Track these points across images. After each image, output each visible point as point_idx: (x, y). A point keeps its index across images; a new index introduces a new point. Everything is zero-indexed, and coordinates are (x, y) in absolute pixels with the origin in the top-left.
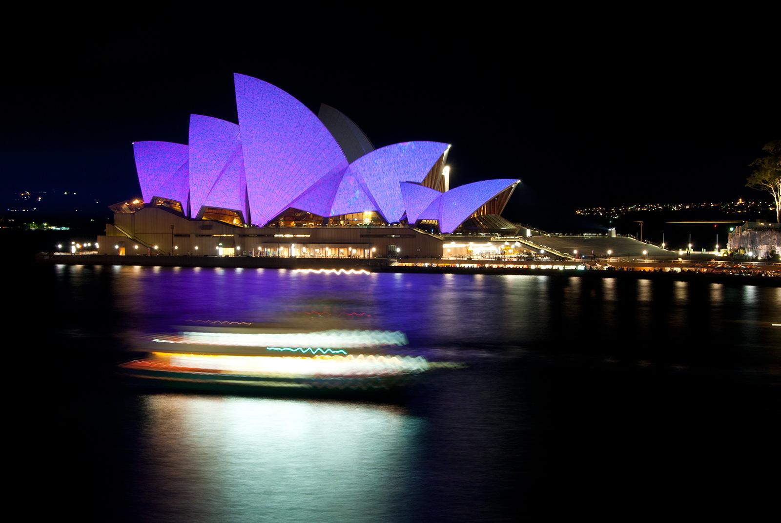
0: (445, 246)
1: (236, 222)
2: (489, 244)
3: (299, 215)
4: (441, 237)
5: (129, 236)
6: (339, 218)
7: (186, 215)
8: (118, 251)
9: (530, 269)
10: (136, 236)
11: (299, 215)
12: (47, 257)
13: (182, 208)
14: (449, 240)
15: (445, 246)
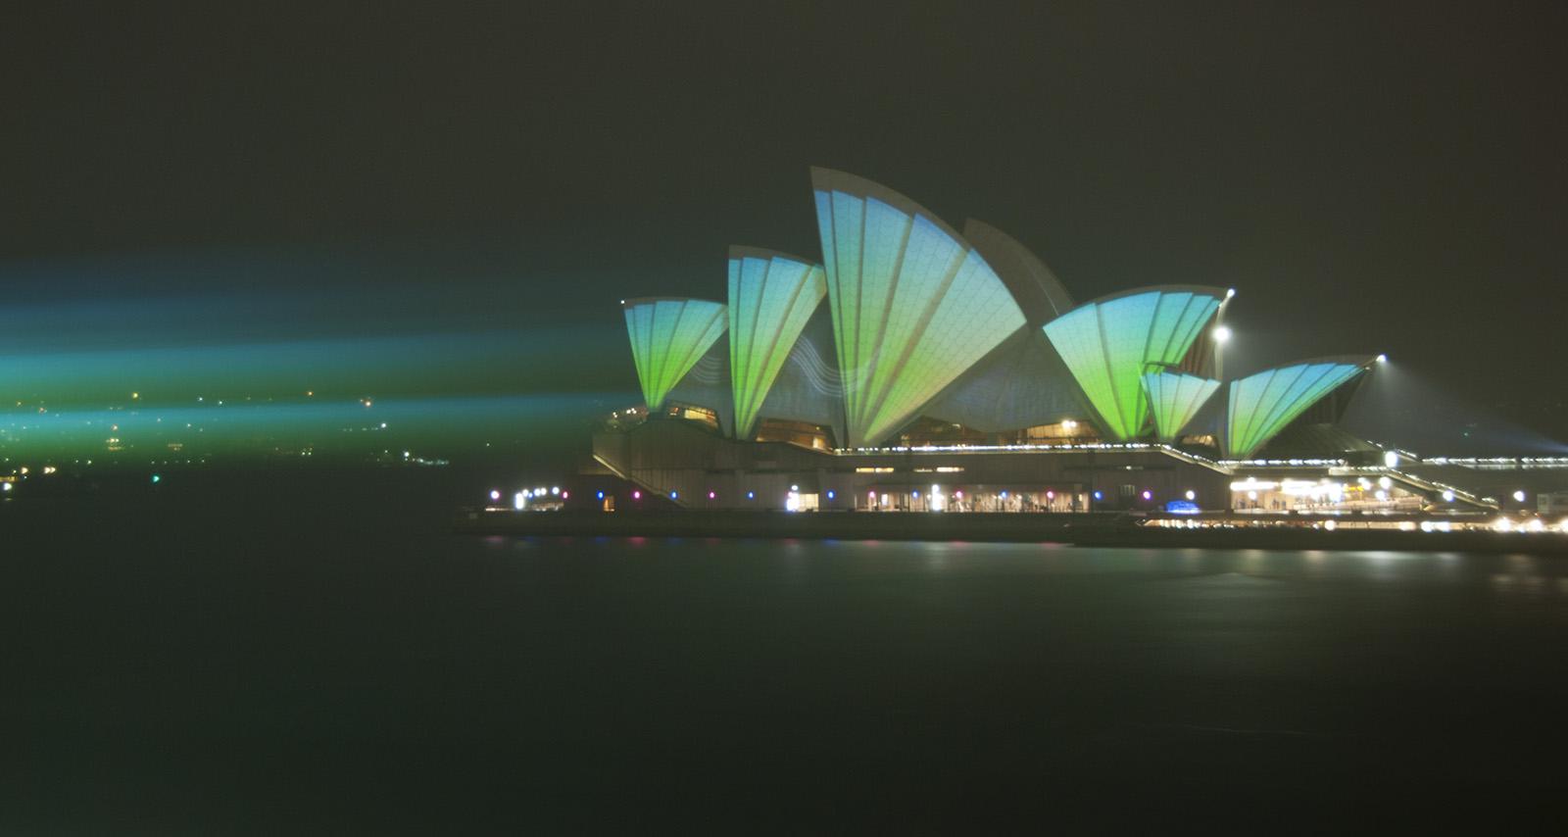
0: (1236, 487)
1: (817, 444)
2: (1325, 481)
3: (939, 430)
4: (1225, 467)
5: (620, 475)
6: (1017, 435)
7: (727, 433)
8: (602, 501)
9: (1421, 530)
10: (634, 473)
11: (939, 430)
12: (474, 516)
13: (718, 420)
14: (1242, 474)
15: (1236, 487)
